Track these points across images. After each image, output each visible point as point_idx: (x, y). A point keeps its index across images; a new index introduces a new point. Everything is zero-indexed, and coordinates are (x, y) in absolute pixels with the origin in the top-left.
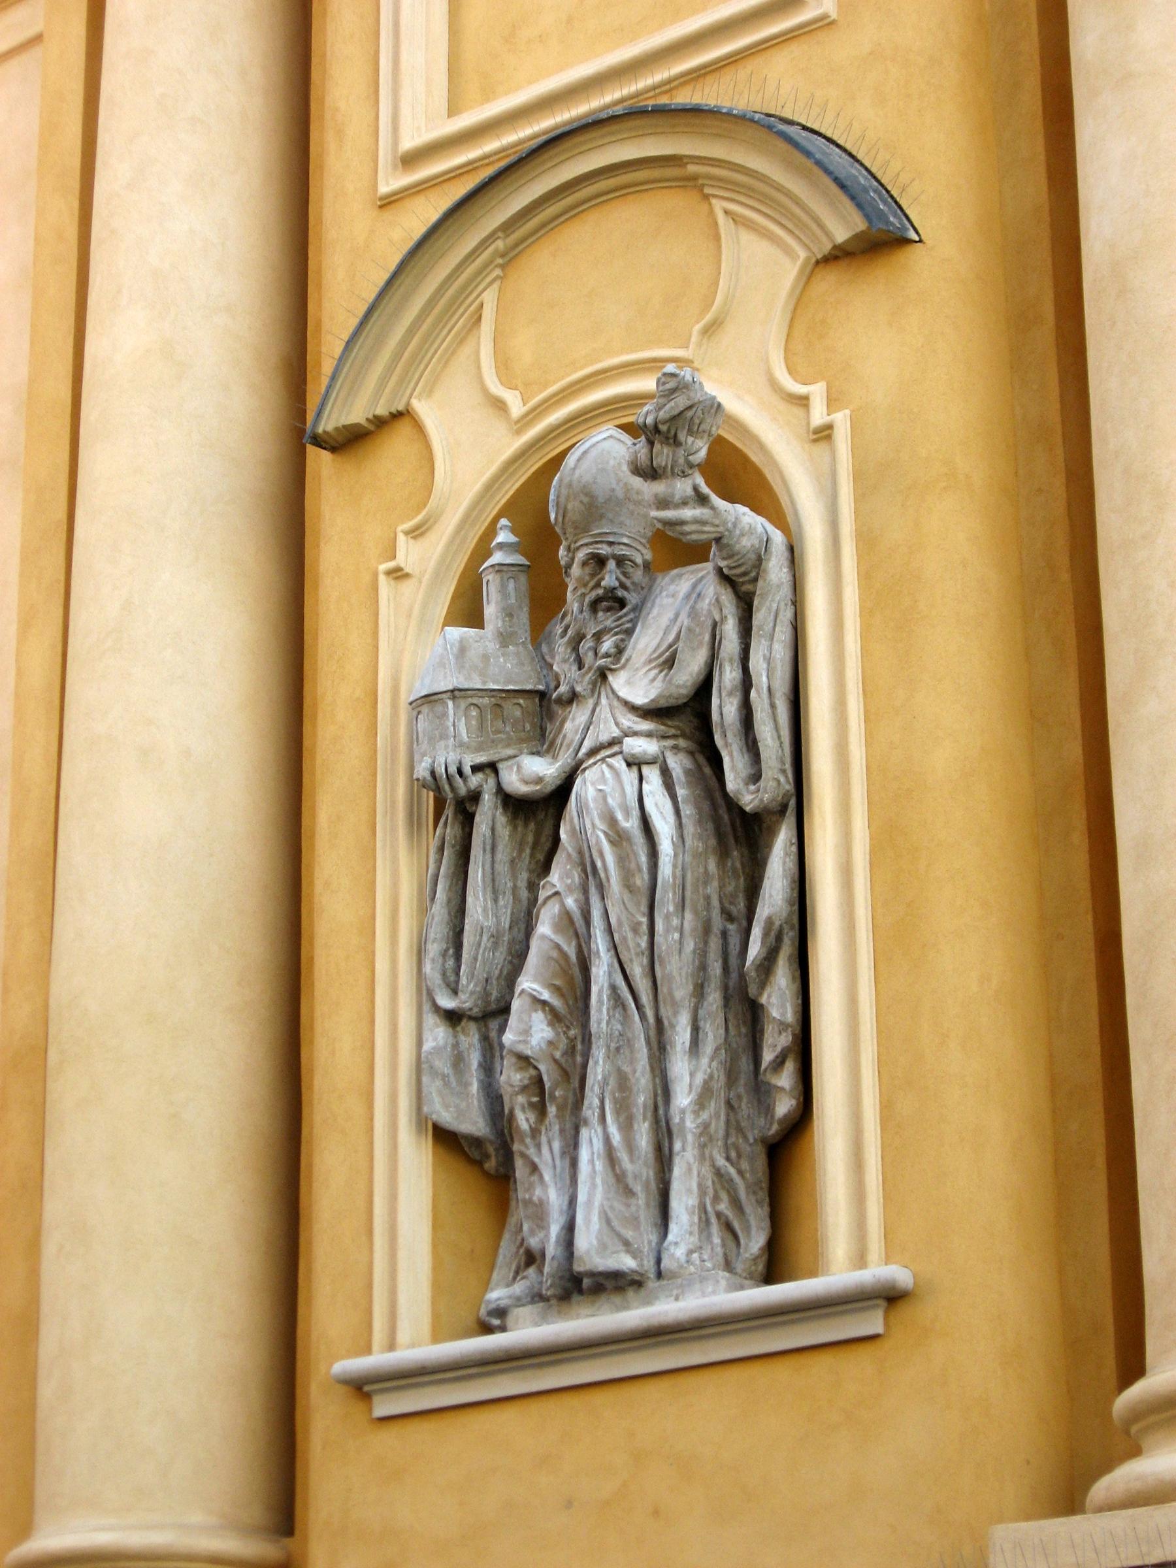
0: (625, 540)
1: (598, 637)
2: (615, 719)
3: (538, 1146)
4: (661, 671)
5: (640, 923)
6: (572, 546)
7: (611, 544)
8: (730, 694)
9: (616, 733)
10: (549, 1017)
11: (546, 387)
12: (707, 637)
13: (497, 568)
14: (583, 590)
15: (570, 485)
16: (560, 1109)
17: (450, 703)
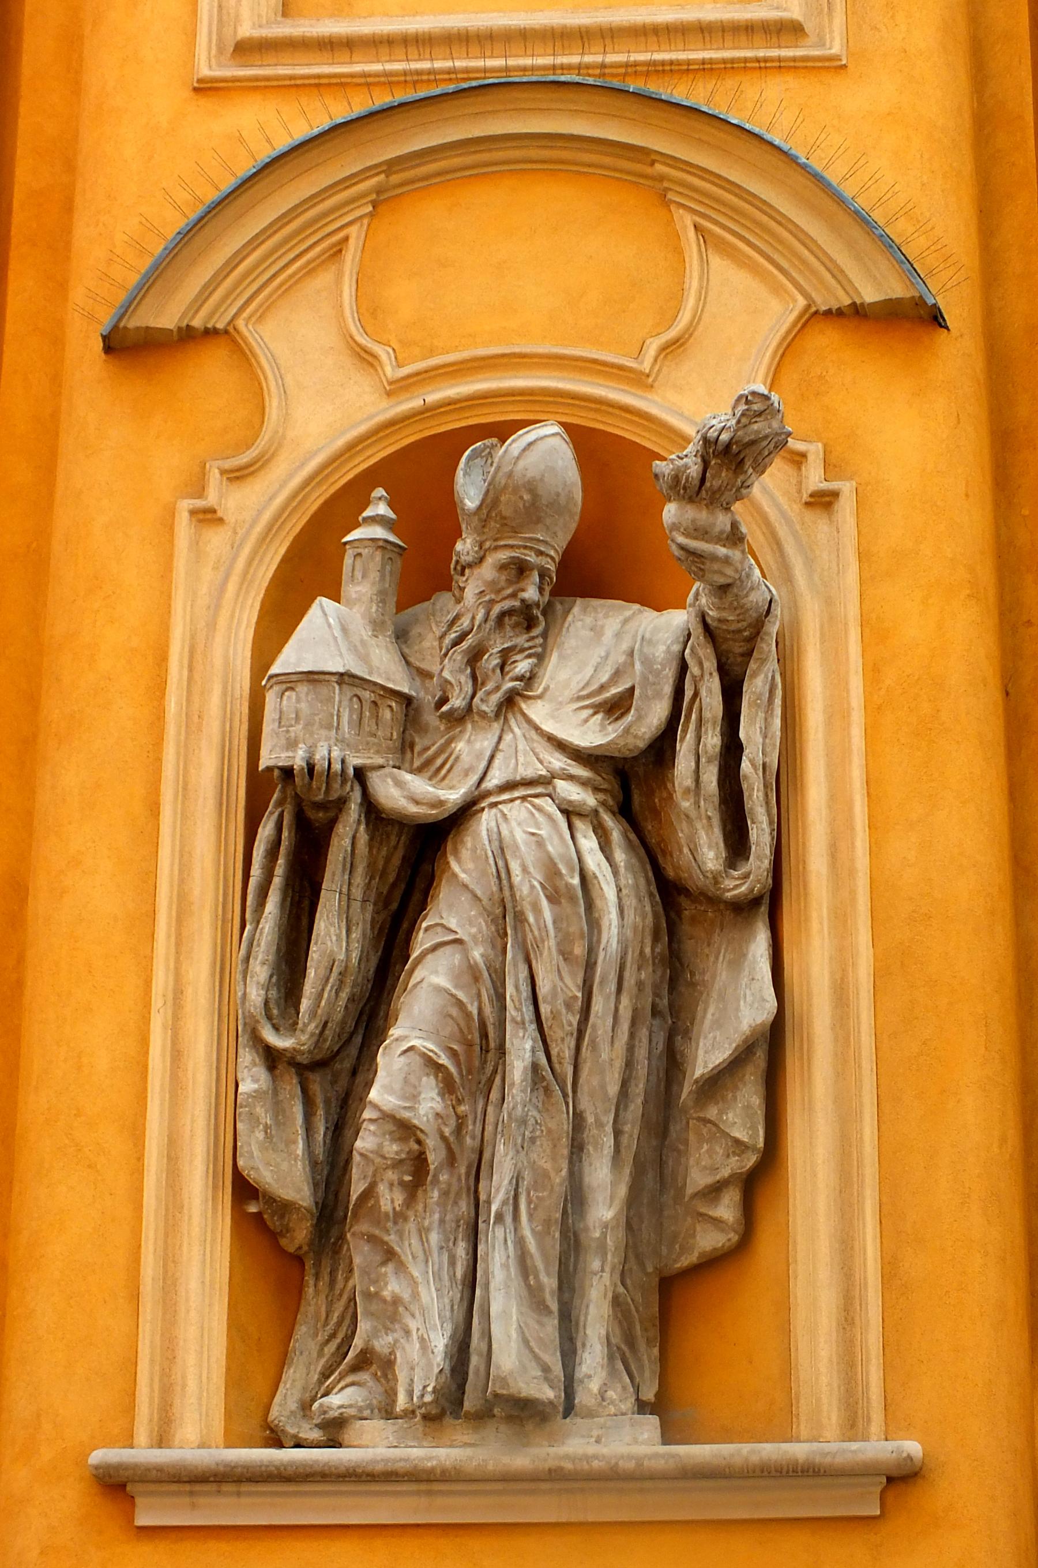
0: (552, 553)
1: (506, 655)
2: (536, 755)
3: (400, 1234)
4: (595, 713)
6: (487, 545)
7: (540, 553)
8: (709, 761)
9: (544, 772)
10: (441, 1085)
11: (431, 352)
12: (668, 689)
13: (381, 543)
14: (493, 596)
15: (510, 475)
16: (445, 1194)
17: (337, 687)
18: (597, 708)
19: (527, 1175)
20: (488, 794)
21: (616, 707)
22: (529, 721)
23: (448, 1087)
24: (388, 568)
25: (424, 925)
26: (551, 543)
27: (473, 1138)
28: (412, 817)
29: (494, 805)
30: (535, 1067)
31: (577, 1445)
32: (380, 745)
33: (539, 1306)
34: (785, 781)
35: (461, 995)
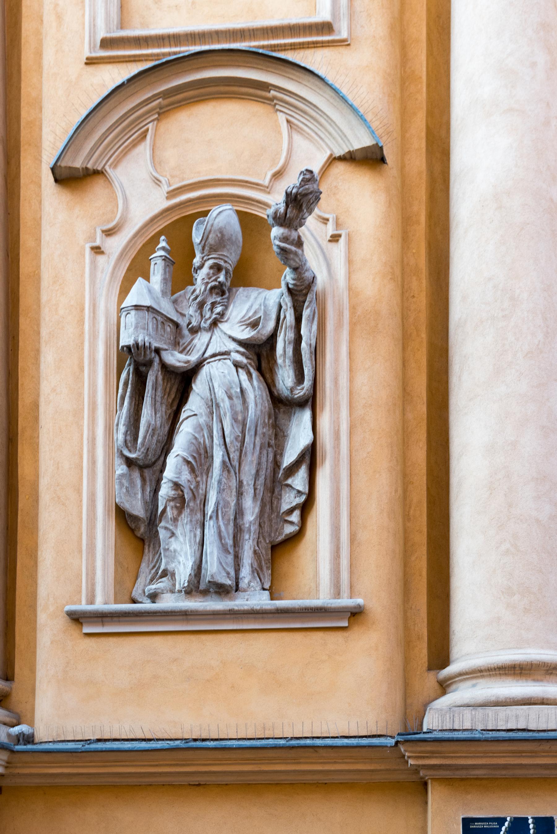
0: (230, 262)
1: (213, 304)
4: (247, 328)
5: (239, 436)
14: (208, 280)
18: (248, 325)
19: (221, 502)
20: (206, 359)
21: (254, 325)
22: (222, 331)
23: (192, 470)
24: (167, 269)
25: (183, 410)
26: (231, 257)
27: (202, 490)
28: (178, 368)
29: (209, 363)
30: (224, 462)
31: (240, 602)
32: (166, 340)
33: (226, 551)
34: (317, 352)
35: (197, 435)
